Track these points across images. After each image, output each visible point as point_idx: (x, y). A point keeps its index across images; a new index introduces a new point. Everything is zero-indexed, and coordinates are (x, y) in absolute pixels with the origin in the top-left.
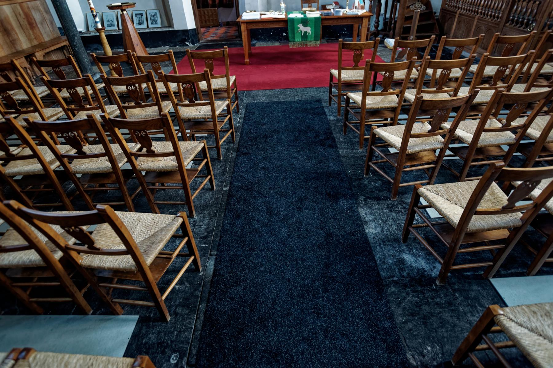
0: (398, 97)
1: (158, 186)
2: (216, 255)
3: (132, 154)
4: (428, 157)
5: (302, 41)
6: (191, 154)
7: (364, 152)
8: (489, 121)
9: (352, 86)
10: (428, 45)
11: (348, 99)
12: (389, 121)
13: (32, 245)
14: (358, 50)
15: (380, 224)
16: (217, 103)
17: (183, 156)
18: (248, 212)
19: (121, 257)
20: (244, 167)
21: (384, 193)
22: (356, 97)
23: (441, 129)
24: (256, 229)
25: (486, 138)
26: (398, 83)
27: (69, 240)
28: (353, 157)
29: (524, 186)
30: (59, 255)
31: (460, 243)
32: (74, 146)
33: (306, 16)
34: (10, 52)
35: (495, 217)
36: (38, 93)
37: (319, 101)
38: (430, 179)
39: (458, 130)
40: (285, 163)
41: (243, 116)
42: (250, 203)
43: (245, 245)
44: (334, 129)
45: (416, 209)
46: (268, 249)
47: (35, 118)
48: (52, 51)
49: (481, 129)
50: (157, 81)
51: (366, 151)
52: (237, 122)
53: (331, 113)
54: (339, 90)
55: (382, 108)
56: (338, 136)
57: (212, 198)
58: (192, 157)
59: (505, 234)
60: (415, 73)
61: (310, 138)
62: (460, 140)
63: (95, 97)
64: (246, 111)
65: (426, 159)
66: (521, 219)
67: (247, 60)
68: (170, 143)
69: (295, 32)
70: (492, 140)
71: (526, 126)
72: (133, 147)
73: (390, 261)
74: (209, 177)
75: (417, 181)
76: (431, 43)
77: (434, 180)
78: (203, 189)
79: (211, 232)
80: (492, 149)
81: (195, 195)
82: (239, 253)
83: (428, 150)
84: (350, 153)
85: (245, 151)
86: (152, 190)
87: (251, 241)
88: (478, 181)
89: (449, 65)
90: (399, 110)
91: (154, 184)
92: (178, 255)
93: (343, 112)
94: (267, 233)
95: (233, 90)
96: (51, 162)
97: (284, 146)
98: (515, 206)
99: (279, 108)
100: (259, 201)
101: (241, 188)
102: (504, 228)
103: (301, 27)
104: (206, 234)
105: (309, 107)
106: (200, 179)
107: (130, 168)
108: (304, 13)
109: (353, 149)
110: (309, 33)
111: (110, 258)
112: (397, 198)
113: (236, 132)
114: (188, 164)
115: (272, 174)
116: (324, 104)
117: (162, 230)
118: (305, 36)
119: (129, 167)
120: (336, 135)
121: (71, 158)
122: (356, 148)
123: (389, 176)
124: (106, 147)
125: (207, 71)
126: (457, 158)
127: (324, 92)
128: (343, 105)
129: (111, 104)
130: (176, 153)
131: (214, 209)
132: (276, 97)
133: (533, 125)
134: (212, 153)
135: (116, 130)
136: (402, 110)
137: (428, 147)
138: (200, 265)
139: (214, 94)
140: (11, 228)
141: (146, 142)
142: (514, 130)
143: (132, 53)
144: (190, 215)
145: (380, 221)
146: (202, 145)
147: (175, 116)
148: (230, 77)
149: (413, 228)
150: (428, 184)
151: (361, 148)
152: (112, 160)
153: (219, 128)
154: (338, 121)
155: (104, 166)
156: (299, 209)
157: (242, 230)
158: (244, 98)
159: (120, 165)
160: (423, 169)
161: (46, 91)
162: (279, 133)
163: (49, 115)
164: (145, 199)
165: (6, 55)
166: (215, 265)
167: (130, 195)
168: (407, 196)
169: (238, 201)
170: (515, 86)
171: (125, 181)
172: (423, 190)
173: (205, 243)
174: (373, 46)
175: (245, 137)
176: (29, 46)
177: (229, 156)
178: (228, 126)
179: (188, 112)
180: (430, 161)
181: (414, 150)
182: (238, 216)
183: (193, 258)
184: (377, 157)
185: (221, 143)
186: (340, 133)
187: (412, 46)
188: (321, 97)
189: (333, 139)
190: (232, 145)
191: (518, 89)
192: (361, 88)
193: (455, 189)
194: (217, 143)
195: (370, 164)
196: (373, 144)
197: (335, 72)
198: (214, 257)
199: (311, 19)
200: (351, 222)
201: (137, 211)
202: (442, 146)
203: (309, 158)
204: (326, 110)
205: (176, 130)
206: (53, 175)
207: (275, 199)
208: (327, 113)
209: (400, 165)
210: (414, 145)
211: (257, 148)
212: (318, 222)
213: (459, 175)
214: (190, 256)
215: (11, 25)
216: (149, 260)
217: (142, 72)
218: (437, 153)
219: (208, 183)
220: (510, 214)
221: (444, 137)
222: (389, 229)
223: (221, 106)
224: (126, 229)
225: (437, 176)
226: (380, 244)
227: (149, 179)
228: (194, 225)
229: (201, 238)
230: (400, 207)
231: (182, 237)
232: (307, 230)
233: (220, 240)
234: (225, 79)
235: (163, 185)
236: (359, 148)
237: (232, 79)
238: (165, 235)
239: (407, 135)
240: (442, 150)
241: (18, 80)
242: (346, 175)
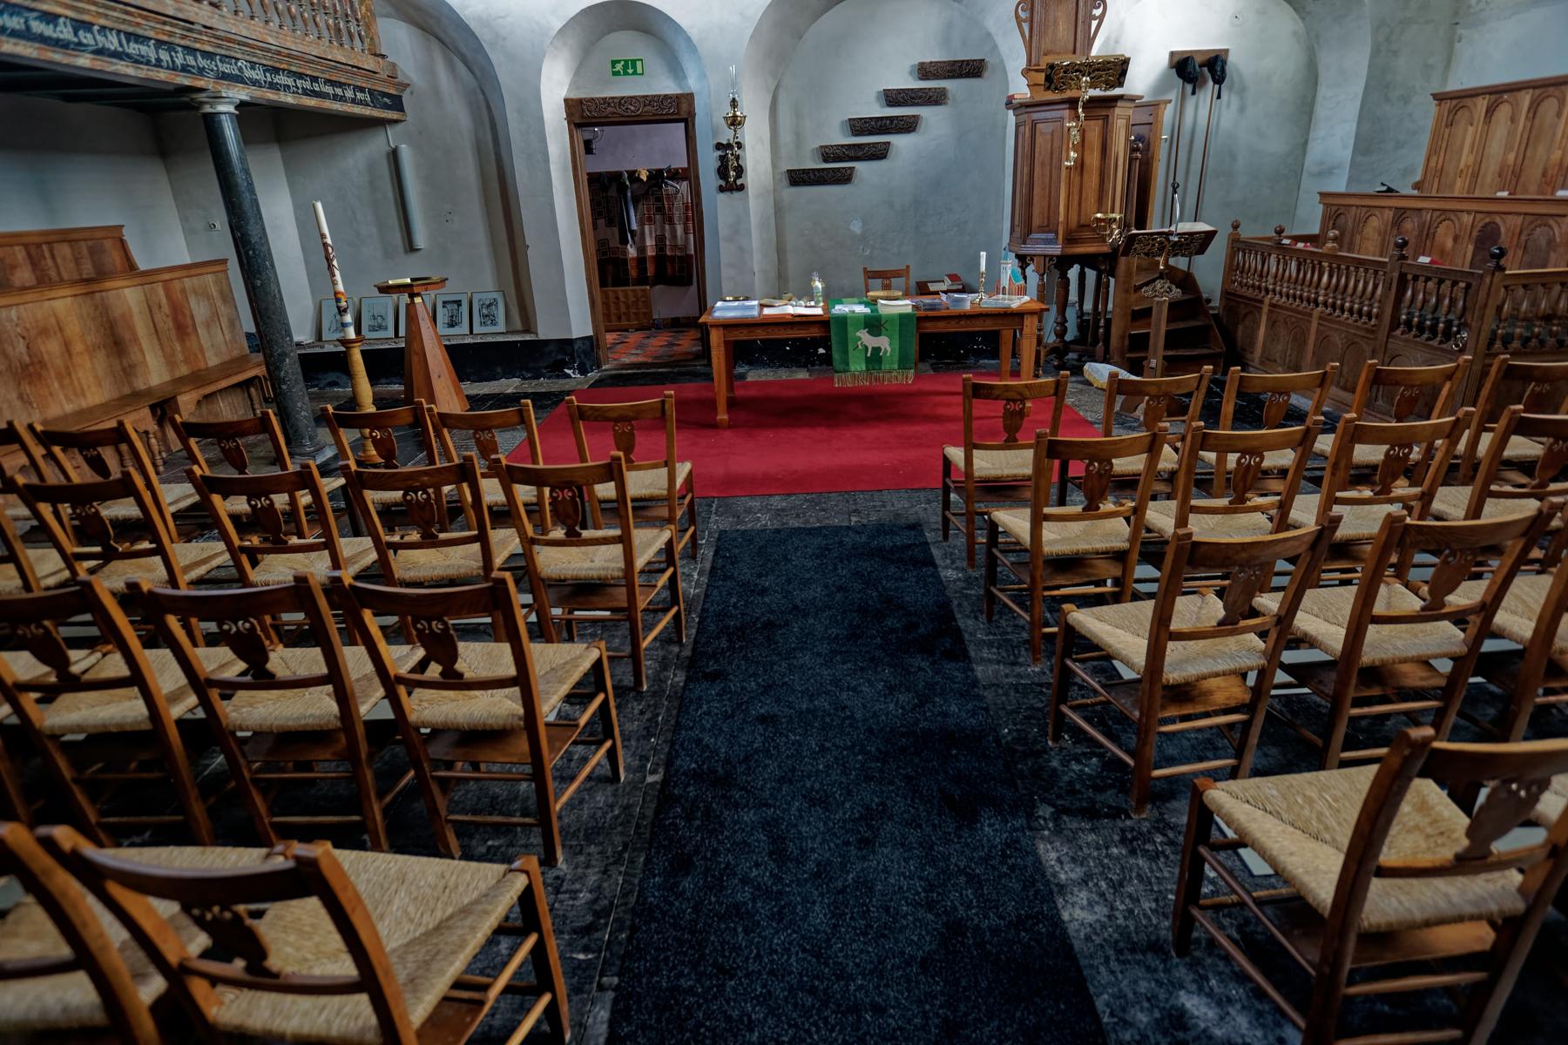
0: (1129, 523)
1: (461, 770)
2: (616, 989)
4: (1228, 692)
5: (868, 370)
6: (561, 682)
7: (1044, 673)
8: (1383, 589)
9: (1003, 490)
10: (1197, 388)
12: (1109, 587)
13: (84, 958)
14: (1014, 401)
15: (1102, 895)
16: (640, 536)
18: (715, 852)
19: (337, 1000)
20: (708, 713)
21: (1110, 797)
22: (1014, 521)
24: (737, 906)
26: (1127, 484)
27: (191, 940)
28: (1016, 688)
29: (1503, 795)
30: (153, 987)
31: (1348, 966)
32: (241, 655)
33: (877, 311)
34: (116, 395)
35: (1440, 883)
36: (169, 500)
37: (916, 527)
38: (1239, 754)
39: (1299, 615)
40: (822, 703)
41: (708, 565)
42: (722, 825)
43: (702, 957)
44: (960, 605)
45: (1203, 851)
46: (772, 973)
47: (149, 574)
48: (220, 391)
50: (484, 476)
51: (1051, 670)
52: (692, 582)
53: (948, 561)
54: (968, 500)
55: (1087, 552)
56: (972, 627)
57: (611, 806)
59: (1480, 936)
60: (1168, 459)
61: (893, 630)
63: (317, 512)
64: (716, 553)
65: (1220, 699)
66: (1521, 890)
67: (723, 416)
68: (506, 648)
69: (851, 348)
70: (1399, 644)
72: (403, 657)
74: (608, 744)
75: (1201, 759)
76: (1205, 383)
77: (1250, 759)
78: (589, 778)
79: (605, 912)
80: (1406, 668)
81: (564, 799)
82: (685, 983)
84: (1007, 676)
85: (712, 666)
86: (445, 784)
87: (722, 943)
89: (1256, 443)
90: (1135, 556)
91: (449, 765)
92: (508, 990)
93: (981, 558)
94: (771, 918)
95: (684, 497)
96: (175, 698)
97: (819, 655)
98: (1490, 853)
99: (806, 547)
100: (749, 817)
101: (697, 776)
102: (1473, 918)
103: (865, 338)
104: (589, 918)
105: (888, 542)
106: (580, 748)
107: (389, 714)
108: (873, 303)
109: (1014, 664)
110: (886, 351)
111: (305, 1002)
112: (1149, 812)
113: (689, 611)
114: (549, 708)
115: (787, 737)
118: (875, 358)
119: (386, 713)
120: (965, 623)
121: (229, 689)
122: (1021, 660)
123: (1120, 746)
124: (331, 658)
125: (619, 459)
126: (1306, 690)
127: (929, 502)
128: (982, 539)
129: (357, 533)
131: (618, 839)
132: (798, 516)
133: (1508, 600)
134: (619, 671)
136: (1141, 554)
138: (566, 1023)
139: (634, 508)
140: (30, 899)
142: (1459, 618)
143: (425, 406)
144: (548, 861)
145: (1103, 884)
147: (524, 569)
148: (677, 465)
149: (1202, 908)
150: (1233, 774)
151: (1036, 660)
153: (642, 603)
154: (969, 581)
155: (318, 712)
156: (865, 843)
157: (696, 910)
158: (714, 518)
159: (363, 709)
160: (1218, 727)
161: (191, 495)
162: (806, 616)
163: (187, 563)
164: (420, 806)
165: (103, 401)
166: (612, 1023)
167: (380, 796)
168: (1175, 804)
169: (689, 818)
170: (1442, 491)
171: (371, 755)
173: (586, 950)
174: (1052, 391)
175: (712, 627)
176: (167, 378)
177: (665, 682)
178: (666, 594)
179: (557, 561)
180: (1233, 703)
181: (1184, 674)
182: (682, 865)
183: (546, 999)
184: (1081, 687)
185: (645, 644)
186: (976, 618)
187: (1153, 390)
188: (922, 515)
189: (957, 634)
190: (676, 649)
191: (1452, 503)
192: (1028, 494)
194: (635, 644)
195: (1064, 709)
196: (1067, 653)
197: (956, 454)
198: (610, 995)
199: (890, 318)
200: (1018, 887)
202: (1263, 662)
203: (891, 689)
204: (935, 552)
205: (524, 606)
206: (173, 734)
207: (793, 811)
208: (939, 562)
209: (1147, 713)
210: (1181, 662)
211: (745, 658)
212: (919, 885)
213: (1320, 742)
214: (538, 994)
215: (132, 329)
217: (450, 459)
218: (1252, 679)
219: (605, 762)
220: (1483, 876)
222: (1131, 911)
223: (649, 542)
224: (367, 917)
225: (1259, 746)
226: (1107, 959)
227: (437, 750)
228: (557, 891)
229: (574, 931)
230: (1159, 839)
231: (523, 933)
232: (887, 910)
233: (629, 939)
234: (664, 471)
235: (476, 767)
236: (1030, 661)
237: (683, 470)
239: (1161, 633)
240: (1263, 674)
241: (126, 475)
242: (997, 740)
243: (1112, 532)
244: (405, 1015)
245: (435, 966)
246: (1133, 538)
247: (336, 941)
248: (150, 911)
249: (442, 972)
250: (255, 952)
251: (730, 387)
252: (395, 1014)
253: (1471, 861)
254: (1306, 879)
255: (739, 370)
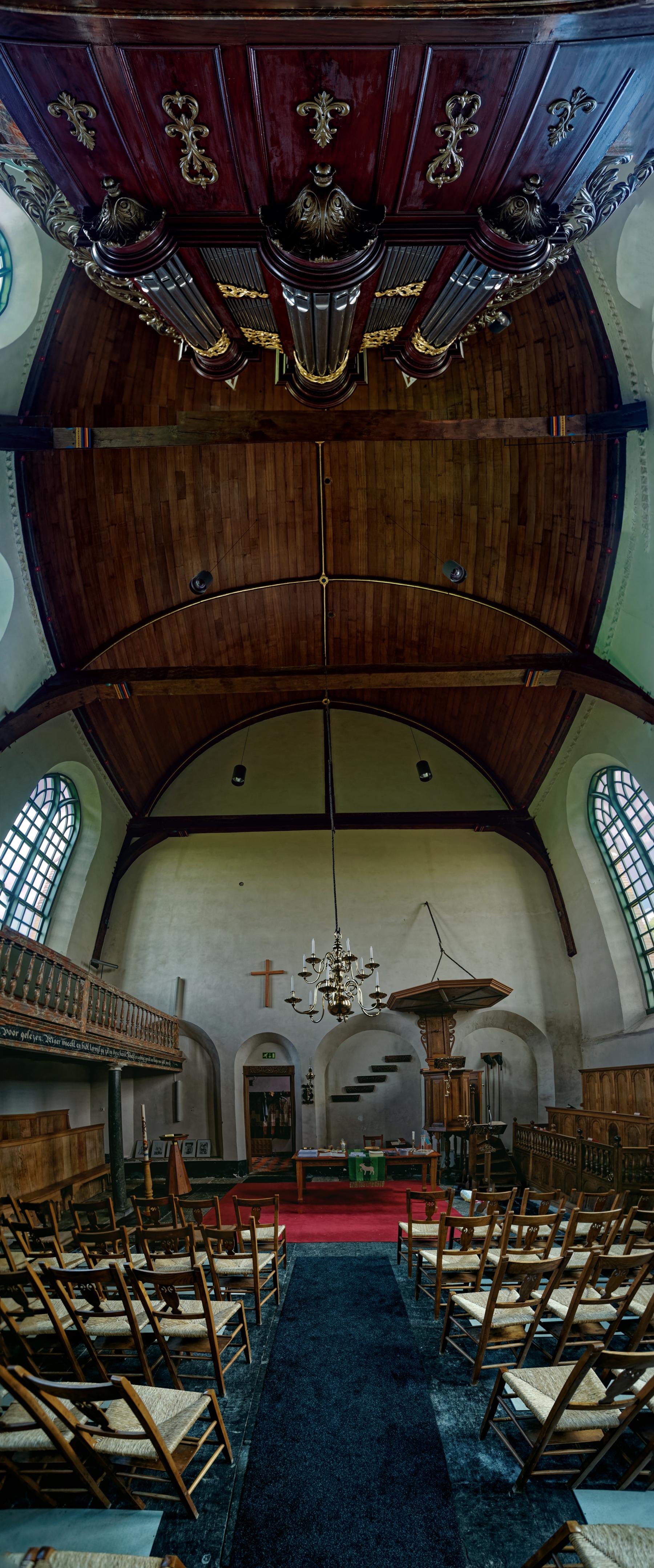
1: (182, 1355)
2: (250, 1445)
3: (155, 1314)
4: (516, 1333)
8: (585, 1291)
11: (421, 1257)
12: (470, 1286)
15: (455, 1416)
17: (214, 1319)
18: (291, 1394)
20: (289, 1335)
21: (463, 1377)
23: (531, 1298)
24: (300, 1416)
25: (584, 1312)
28: (427, 1329)
32: (90, 1301)
37: (386, 1258)
38: (518, 1361)
39: (550, 1300)
40: (341, 1332)
41: (291, 1272)
42: (294, 1382)
43: (286, 1434)
45: (499, 1398)
46: (315, 1441)
47: (52, 1263)
49: (576, 1301)
52: (283, 1279)
55: (461, 1270)
56: (409, 1302)
57: (246, 1374)
58: (225, 1320)
61: (374, 1302)
62: (553, 1313)
64: (295, 1266)
65: (513, 1336)
68: (200, 1303)
70: (590, 1314)
71: (629, 1298)
72: (157, 1306)
73: (463, 1462)
74: (245, 1347)
75: (502, 1362)
77: (522, 1363)
78: (236, 1361)
79: (245, 1416)
80: (590, 1325)
81: (226, 1369)
82: (279, 1444)
83: (516, 1324)
85: (291, 1315)
86: (176, 1361)
87: (294, 1429)
88: (573, 1366)
90: (482, 1273)
91: (178, 1353)
92: (205, 1443)
93: (414, 1272)
94: (315, 1420)
96: (64, 1320)
100: (306, 1380)
101: (283, 1362)
104: (238, 1418)
105: (373, 1264)
106: (233, 1349)
107: (151, 1331)
109: (427, 1319)
112: (478, 1384)
113: (281, 1291)
114: (220, 1329)
116: (392, 1262)
117: (186, 1410)
119: (150, 1330)
120: (406, 1301)
121: (86, 1316)
123: (469, 1355)
126: (550, 1335)
128: (415, 1264)
130: (206, 1315)
131: (249, 1387)
133: (637, 1296)
134: (250, 1316)
135: (140, 1283)
136: (485, 1273)
137: (516, 1321)
138: (231, 1456)
141: (172, 1300)
142: (615, 1303)
144: (220, 1394)
145: (456, 1412)
146: (239, 1306)
147: (210, 1270)
149: (494, 1422)
150: (515, 1367)
152: (132, 1321)
153: (260, 1286)
154: (409, 1283)
156: (357, 1392)
157: (282, 1416)
159: (141, 1327)
160: (510, 1348)
162: (335, 1294)
164: (167, 1371)
166: (249, 1457)
167: (150, 1366)
168: (489, 1381)
169: (279, 1379)
170: (613, 1247)
171: (145, 1348)
172: (509, 1375)
173: (237, 1430)
175: (292, 1298)
178: (272, 1284)
179: (225, 1265)
180: (518, 1338)
182: (278, 1398)
183: (222, 1446)
184: (455, 1330)
185: (261, 1304)
189: (403, 1306)
190: (275, 1307)
191: (617, 1251)
193: (546, 1375)
194: (257, 1304)
195: (448, 1339)
196: (450, 1313)
198: (248, 1447)
200: (421, 1412)
201: (158, 1385)
203: (372, 1327)
204: (394, 1269)
206: (64, 1335)
207: (326, 1378)
208: (395, 1273)
209: (483, 1341)
211: (306, 1312)
212: (379, 1410)
213: (551, 1357)
214: (219, 1444)
216: (171, 1447)
218: (527, 1329)
219: (243, 1355)
221: (534, 1308)
222: (465, 1422)
223: (265, 1259)
225: (527, 1358)
226: (453, 1440)
227: (173, 1346)
228: (225, 1407)
229: (232, 1423)
230: (481, 1395)
231: (210, 1421)
232: (365, 1419)
233: (255, 1426)
235: (188, 1354)
238: (189, 1417)
240: (533, 1326)
242: (418, 1351)
243: (472, 1261)
244: (166, 1448)
245: (176, 1431)
246: (481, 1265)
247: (136, 1420)
248: (60, 1404)
249: (179, 1433)
250: (104, 1423)
251: (304, 1185)
252: (162, 1447)
253: (605, 1404)
254: (538, 1409)
255: (309, 1177)
